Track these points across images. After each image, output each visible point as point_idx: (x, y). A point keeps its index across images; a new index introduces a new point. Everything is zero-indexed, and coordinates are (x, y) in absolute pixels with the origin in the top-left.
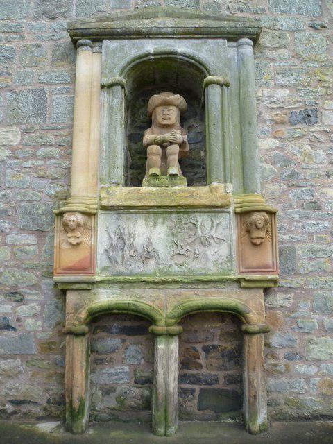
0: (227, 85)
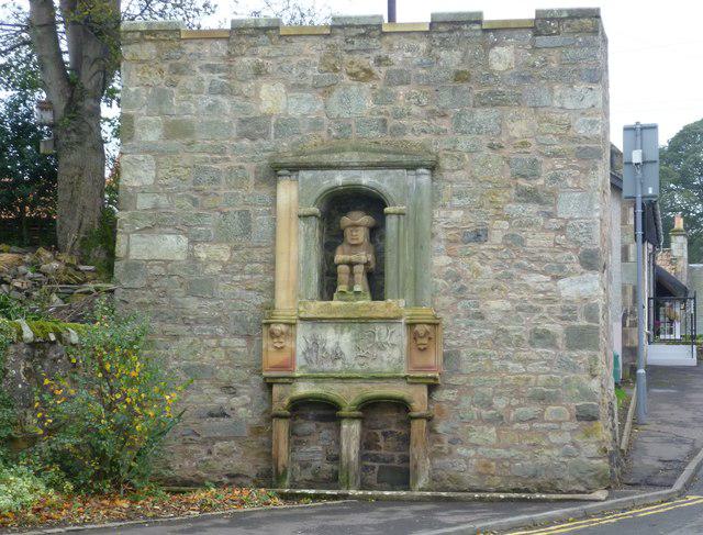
0: (404, 214)
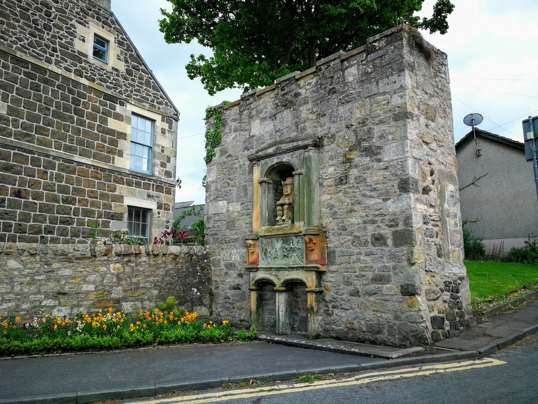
0: (302, 174)
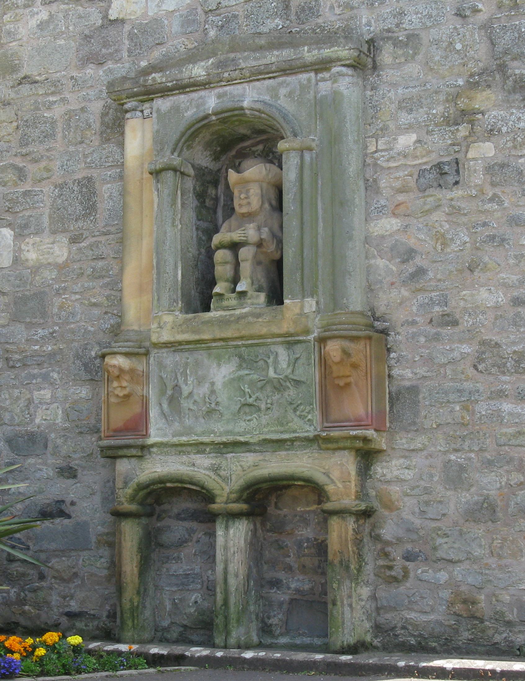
0: (310, 149)
